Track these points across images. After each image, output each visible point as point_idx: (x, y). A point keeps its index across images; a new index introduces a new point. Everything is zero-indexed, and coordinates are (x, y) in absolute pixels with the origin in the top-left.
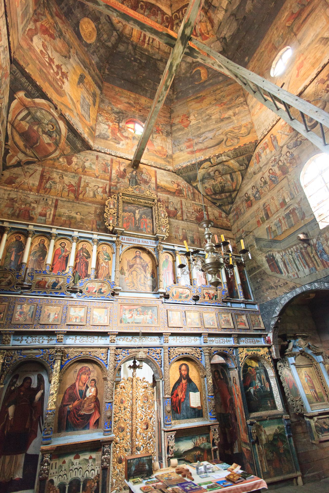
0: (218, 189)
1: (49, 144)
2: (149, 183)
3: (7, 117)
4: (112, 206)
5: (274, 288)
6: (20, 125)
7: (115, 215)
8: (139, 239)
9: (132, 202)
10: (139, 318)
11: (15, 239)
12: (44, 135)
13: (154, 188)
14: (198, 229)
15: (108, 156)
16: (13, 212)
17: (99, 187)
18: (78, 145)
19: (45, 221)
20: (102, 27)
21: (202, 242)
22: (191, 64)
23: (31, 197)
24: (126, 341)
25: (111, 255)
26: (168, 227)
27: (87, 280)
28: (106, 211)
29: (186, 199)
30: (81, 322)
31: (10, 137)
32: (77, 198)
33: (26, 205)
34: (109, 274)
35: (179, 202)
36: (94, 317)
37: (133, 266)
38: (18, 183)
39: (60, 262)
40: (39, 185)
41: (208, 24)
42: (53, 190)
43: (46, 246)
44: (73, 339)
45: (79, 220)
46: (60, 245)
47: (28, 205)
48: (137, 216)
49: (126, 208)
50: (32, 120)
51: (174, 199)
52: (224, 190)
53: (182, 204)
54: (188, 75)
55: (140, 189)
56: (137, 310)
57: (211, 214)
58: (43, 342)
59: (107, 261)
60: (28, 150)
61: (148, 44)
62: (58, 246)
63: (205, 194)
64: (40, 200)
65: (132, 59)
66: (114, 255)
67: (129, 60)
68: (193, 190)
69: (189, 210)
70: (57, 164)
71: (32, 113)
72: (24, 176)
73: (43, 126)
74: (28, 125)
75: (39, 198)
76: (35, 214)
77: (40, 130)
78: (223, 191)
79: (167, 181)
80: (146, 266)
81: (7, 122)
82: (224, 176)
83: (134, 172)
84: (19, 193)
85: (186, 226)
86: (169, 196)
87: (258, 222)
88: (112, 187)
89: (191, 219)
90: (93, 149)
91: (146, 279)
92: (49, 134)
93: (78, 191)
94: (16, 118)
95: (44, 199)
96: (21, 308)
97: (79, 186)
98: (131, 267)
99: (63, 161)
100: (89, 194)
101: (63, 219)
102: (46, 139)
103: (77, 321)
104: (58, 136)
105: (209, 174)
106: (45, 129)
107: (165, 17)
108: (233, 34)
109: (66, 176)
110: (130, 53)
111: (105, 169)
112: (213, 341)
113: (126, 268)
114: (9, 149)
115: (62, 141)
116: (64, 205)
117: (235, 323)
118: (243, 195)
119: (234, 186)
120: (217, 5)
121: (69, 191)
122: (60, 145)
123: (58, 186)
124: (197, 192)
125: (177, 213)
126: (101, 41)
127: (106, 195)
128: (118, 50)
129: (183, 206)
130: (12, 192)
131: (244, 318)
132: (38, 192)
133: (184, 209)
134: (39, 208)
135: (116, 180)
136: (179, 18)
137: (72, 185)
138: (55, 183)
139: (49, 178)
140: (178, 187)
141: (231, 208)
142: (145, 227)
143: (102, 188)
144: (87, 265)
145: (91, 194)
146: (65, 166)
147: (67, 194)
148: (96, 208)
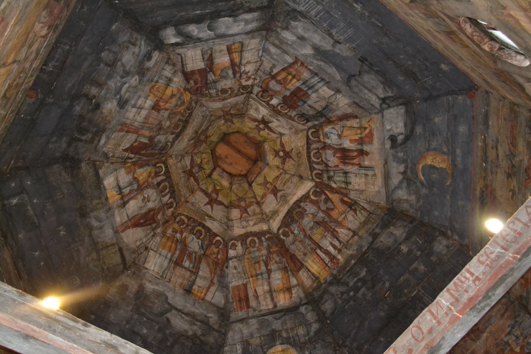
20: (287, 331)
22: (404, 178)
41: (349, 123)
54: (424, 191)
61: (340, 251)
65: (352, 294)
67: (352, 303)
107: (312, 197)
108: (382, 83)
110: (342, 293)
120: (324, 104)
126: (305, 343)
128: (329, 312)
136: (322, 171)
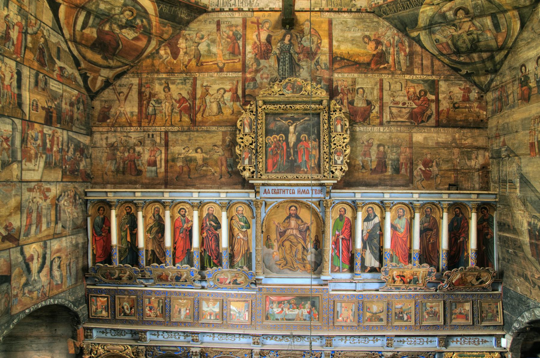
0: (464, 45)
1: (136, 39)
2: (316, 54)
3: (63, 35)
4: (247, 130)
5: (530, 283)
6: (85, 36)
7: (253, 147)
8: (292, 188)
9: (281, 111)
10: (290, 313)
11: (125, 212)
12: (124, 31)
13: (325, 64)
14: (411, 138)
15: (237, 15)
16: (117, 165)
17: (225, 91)
18: (183, 16)
19: (157, 173)
21: (414, 167)
23: (133, 137)
24: (275, 340)
25: (249, 219)
26: (348, 151)
27: (216, 270)
28: (239, 141)
29: (393, 74)
30: (216, 319)
31: (79, 58)
32: (193, 121)
33: (129, 153)
34: (248, 249)
35: (375, 85)
36: (232, 312)
37: (285, 232)
38: (114, 116)
39: (182, 238)
40: (138, 112)
42: (159, 116)
43: (162, 216)
44: (210, 336)
45: (200, 162)
46: (179, 212)
47: (131, 151)
48: (292, 139)
49: (272, 126)
50: (97, 21)
51: (366, 80)
52: (477, 47)
53: (381, 89)
55: (293, 85)
56: (289, 302)
57: (444, 98)
58: (179, 338)
59: (244, 230)
60: (111, 61)
62: (177, 215)
63: (436, 53)
64: (144, 138)
66: (254, 220)
68: (410, 46)
69: (397, 99)
70: (157, 62)
71: (93, 11)
72: (117, 102)
73: (115, 19)
74: (95, 30)
75: (142, 135)
76: (143, 164)
77: (115, 26)
78: (474, 47)
79: (353, 41)
80: (306, 231)
81: (66, 42)
82: (478, 19)
83: (288, 37)
84: (118, 134)
85: (386, 136)
86: (356, 75)
87: (532, 145)
88: (246, 84)
89: (399, 119)
90: (210, 9)
91: (305, 253)
92: (130, 25)
93: (194, 108)
94: (74, 30)
95: (149, 135)
96: (150, 303)
97: (195, 98)
98: (282, 234)
99: (166, 53)
100: (211, 108)
101: (179, 164)
102: (129, 34)
103: (212, 318)
104: (144, 20)
105: (443, 16)
106: (121, 21)
109: (173, 83)
111: (234, 48)
112: (404, 342)
113: (274, 236)
114: (86, 73)
115: (154, 23)
116: (177, 140)
117: (448, 315)
118: (518, 65)
119: (500, 39)
121: (181, 111)
122: (153, 31)
123: (163, 105)
124: (418, 49)
125: (371, 111)
127: (238, 103)
129: (385, 93)
130: (109, 135)
131: (468, 307)
132: (140, 126)
133: (387, 98)
134: (146, 152)
135: (255, 67)
137: (184, 98)
138: (159, 102)
139: (152, 95)
140: (376, 48)
141: (492, 80)
142: (304, 158)
143: (230, 90)
144: (217, 239)
145: (214, 106)
146: (170, 63)
147: (179, 117)
148: (224, 133)
